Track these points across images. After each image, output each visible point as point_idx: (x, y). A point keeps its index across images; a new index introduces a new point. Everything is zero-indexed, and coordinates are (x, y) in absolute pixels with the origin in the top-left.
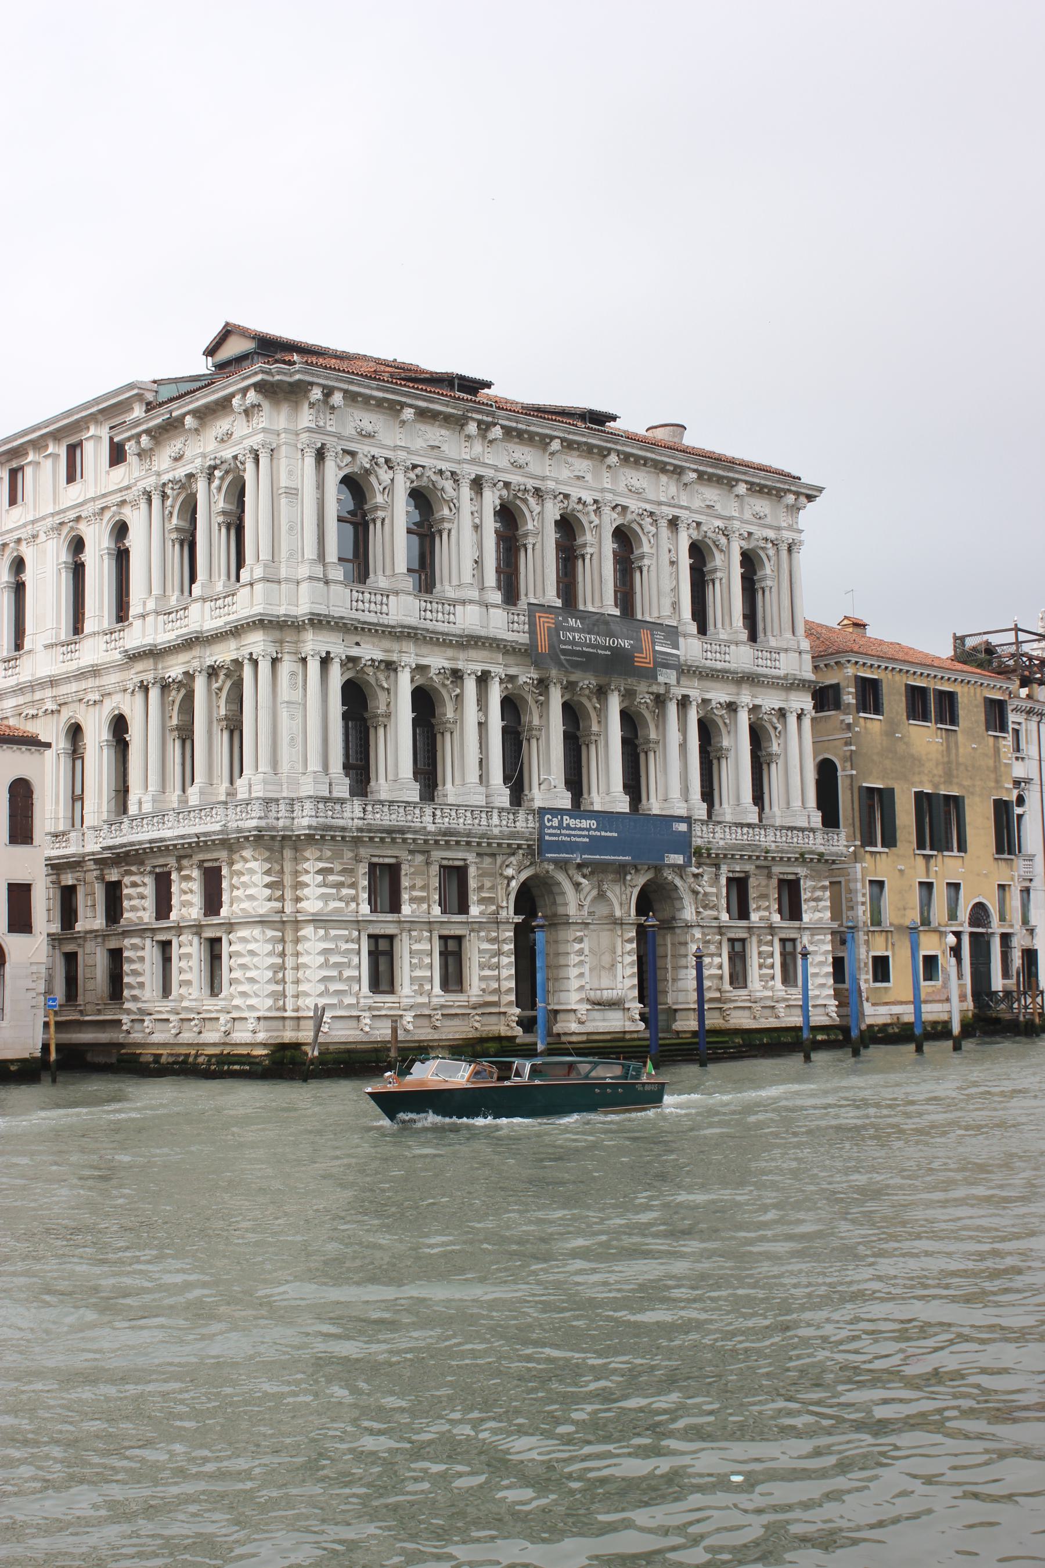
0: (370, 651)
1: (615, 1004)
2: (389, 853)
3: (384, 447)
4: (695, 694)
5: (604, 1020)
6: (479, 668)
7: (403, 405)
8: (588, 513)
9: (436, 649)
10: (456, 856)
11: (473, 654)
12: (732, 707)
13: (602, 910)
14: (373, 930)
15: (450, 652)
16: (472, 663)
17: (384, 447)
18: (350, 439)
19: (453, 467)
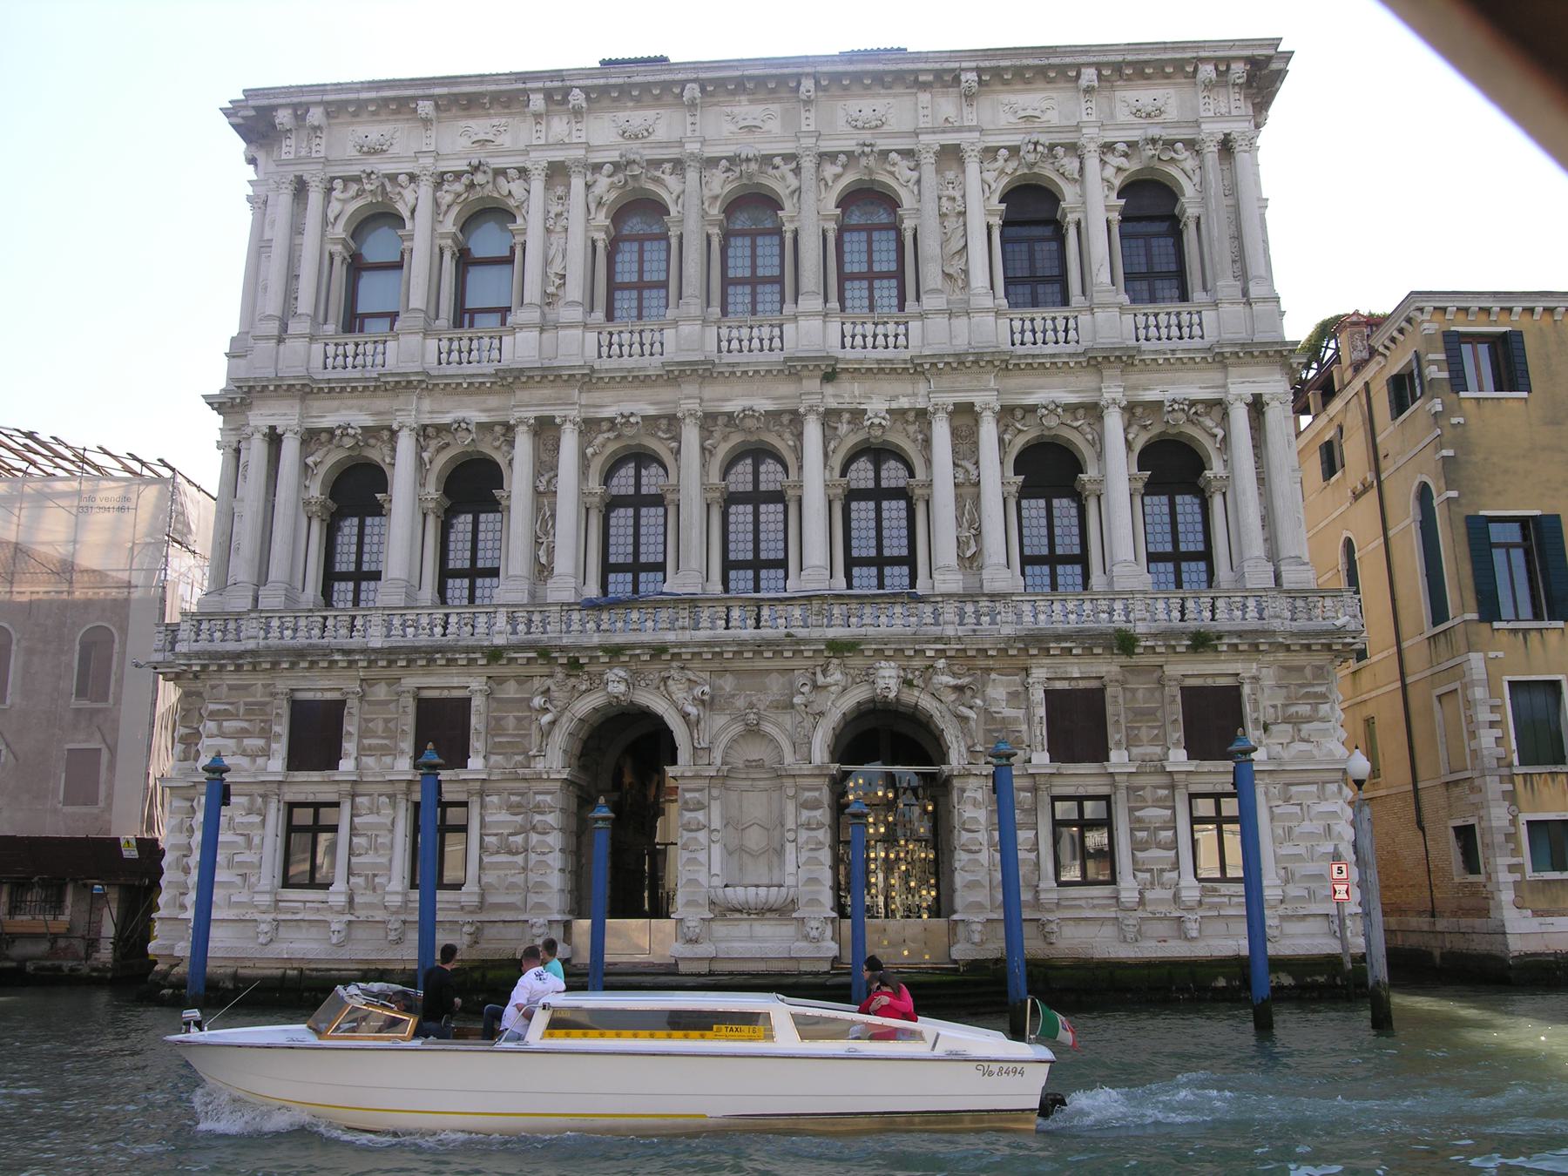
0: (354, 416)
1: (782, 911)
2: (326, 684)
3: (398, 159)
4: (986, 397)
5: (752, 938)
6: (531, 414)
7: (415, 99)
8: (783, 178)
9: (466, 399)
10: (442, 682)
11: (522, 395)
12: (1094, 411)
13: (755, 751)
14: (290, 796)
15: (493, 401)
16: (524, 408)
17: (398, 159)
18: (349, 162)
19: (517, 161)
